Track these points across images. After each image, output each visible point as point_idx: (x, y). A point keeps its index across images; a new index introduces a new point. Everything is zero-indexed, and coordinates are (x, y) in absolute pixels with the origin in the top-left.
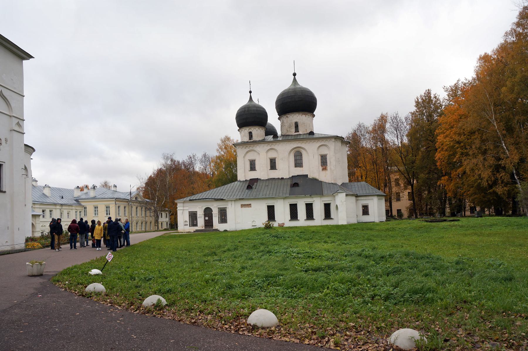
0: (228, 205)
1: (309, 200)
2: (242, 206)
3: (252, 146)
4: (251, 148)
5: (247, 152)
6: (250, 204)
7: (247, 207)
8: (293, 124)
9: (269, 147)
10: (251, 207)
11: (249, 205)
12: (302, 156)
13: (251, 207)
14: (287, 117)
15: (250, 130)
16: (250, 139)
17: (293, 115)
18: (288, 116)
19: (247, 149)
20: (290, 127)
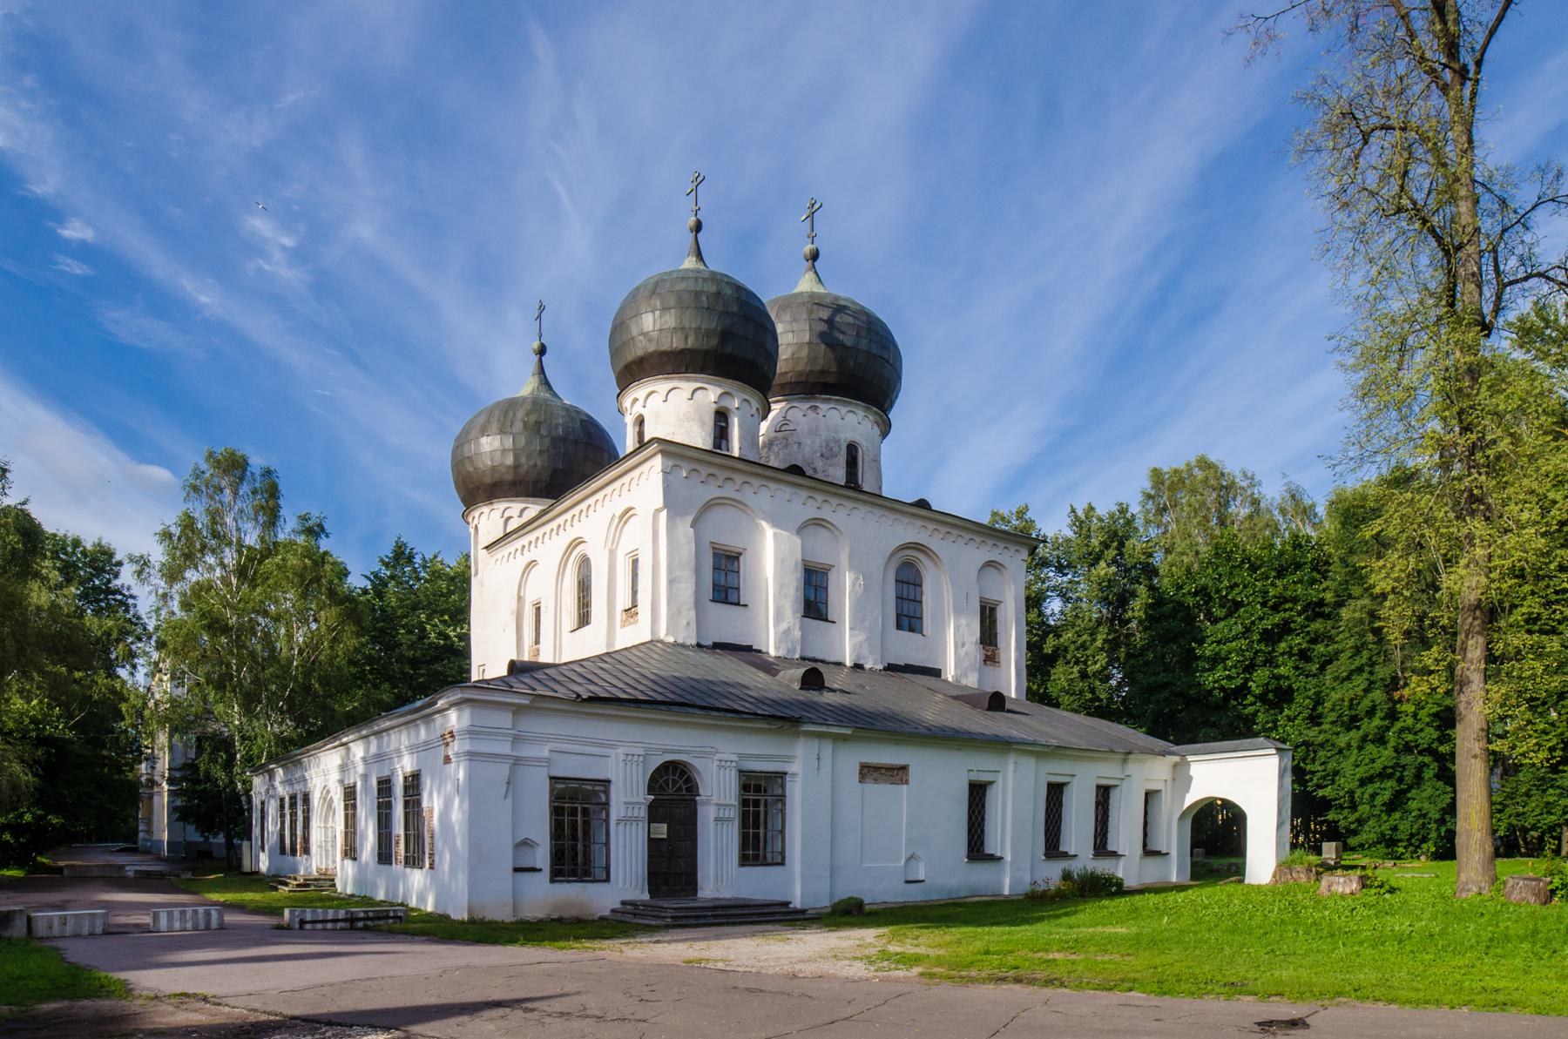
0: (790, 759)
1: (1107, 771)
2: (869, 772)
3: (739, 478)
4: (729, 491)
5: (709, 505)
6: (904, 768)
7: (885, 782)
8: (839, 446)
9: (811, 512)
10: (907, 782)
11: (898, 774)
12: (921, 586)
13: (907, 782)
14: (814, 408)
15: (726, 403)
16: (717, 445)
17: (844, 410)
18: (824, 407)
19: (711, 491)
20: (827, 455)
